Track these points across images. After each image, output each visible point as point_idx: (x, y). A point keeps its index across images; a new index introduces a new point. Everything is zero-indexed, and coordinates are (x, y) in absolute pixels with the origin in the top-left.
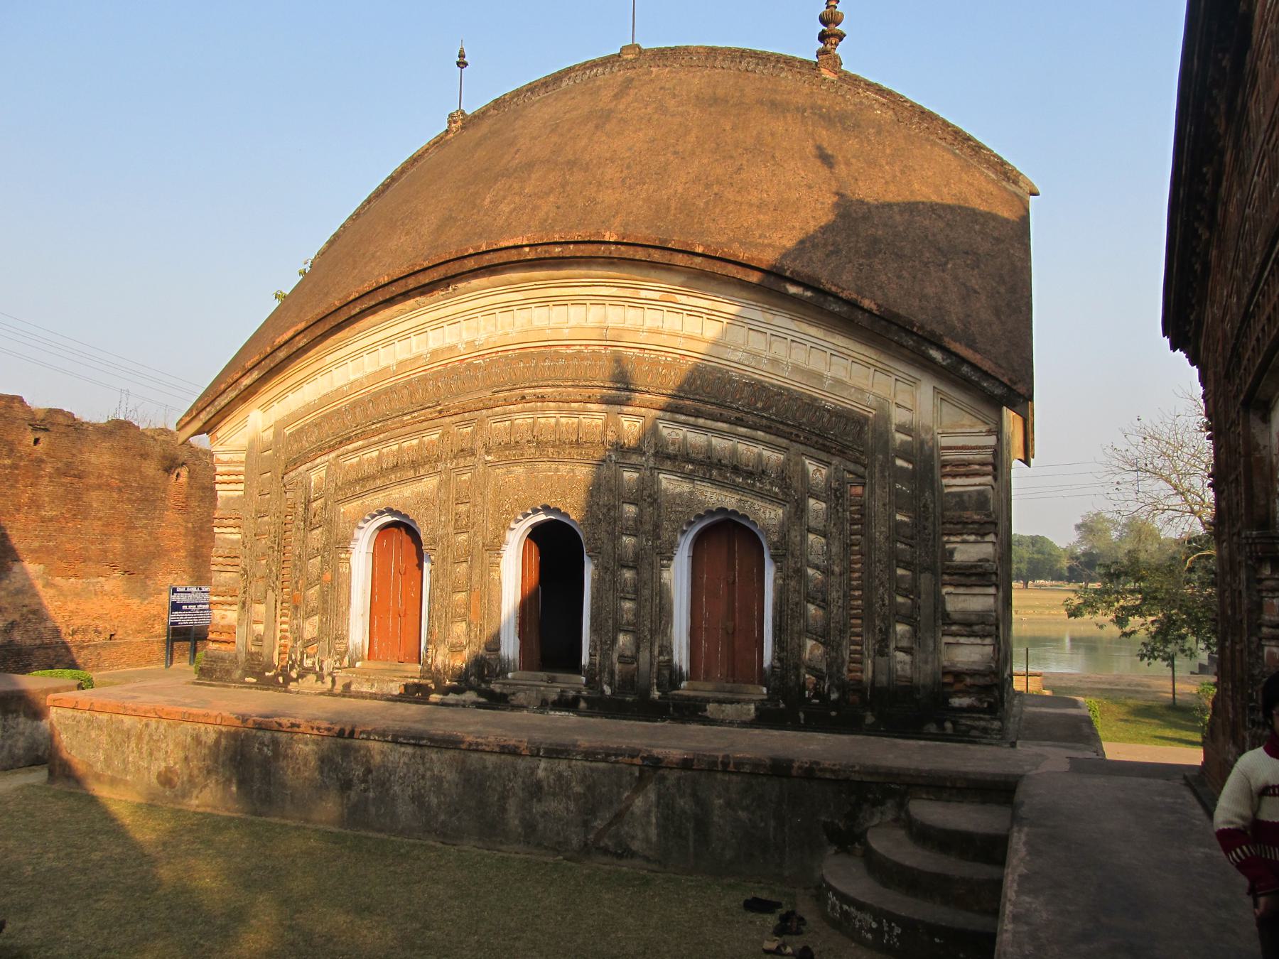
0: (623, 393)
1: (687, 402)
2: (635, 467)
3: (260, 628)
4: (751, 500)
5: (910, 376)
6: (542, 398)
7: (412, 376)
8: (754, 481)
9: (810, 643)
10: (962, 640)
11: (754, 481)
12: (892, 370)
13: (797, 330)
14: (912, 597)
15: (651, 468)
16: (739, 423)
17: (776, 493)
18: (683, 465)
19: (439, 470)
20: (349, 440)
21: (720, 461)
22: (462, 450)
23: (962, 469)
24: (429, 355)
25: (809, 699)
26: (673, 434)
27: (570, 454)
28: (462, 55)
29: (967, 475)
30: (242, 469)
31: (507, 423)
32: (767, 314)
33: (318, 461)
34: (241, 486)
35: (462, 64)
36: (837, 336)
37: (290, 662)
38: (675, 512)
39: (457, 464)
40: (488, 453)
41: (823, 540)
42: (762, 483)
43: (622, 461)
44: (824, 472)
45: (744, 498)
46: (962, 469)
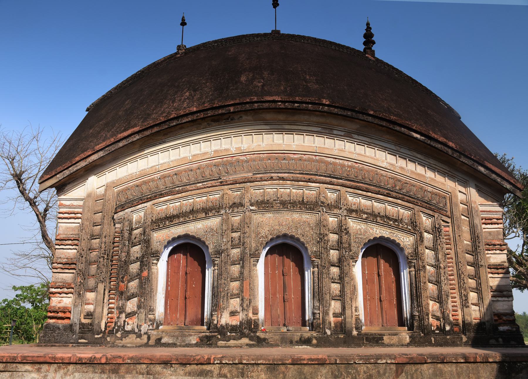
0: (327, 178)
1: (361, 185)
2: (336, 215)
3: (91, 308)
4: (397, 233)
5: (463, 178)
6: (283, 179)
7: (201, 163)
8: (399, 223)
9: (431, 303)
10: (500, 299)
11: (399, 223)
12: (456, 176)
13: (412, 155)
14: (476, 279)
15: (345, 216)
16: (389, 195)
17: (410, 229)
18: (362, 214)
19: (221, 213)
20: (162, 195)
21: (379, 213)
22: (234, 204)
23: (489, 221)
24: (213, 153)
25: (434, 331)
26: (354, 200)
27: (300, 207)
28: (183, 19)
29: (492, 224)
30: (80, 210)
31: (261, 190)
32: (397, 147)
33: (140, 206)
34: (79, 221)
35: (183, 24)
36: (431, 159)
37: (116, 328)
38: (358, 238)
39: (233, 211)
40: (252, 205)
41: (433, 252)
42: (402, 224)
43: (330, 212)
44: (430, 220)
45: (393, 232)
46: (489, 221)
